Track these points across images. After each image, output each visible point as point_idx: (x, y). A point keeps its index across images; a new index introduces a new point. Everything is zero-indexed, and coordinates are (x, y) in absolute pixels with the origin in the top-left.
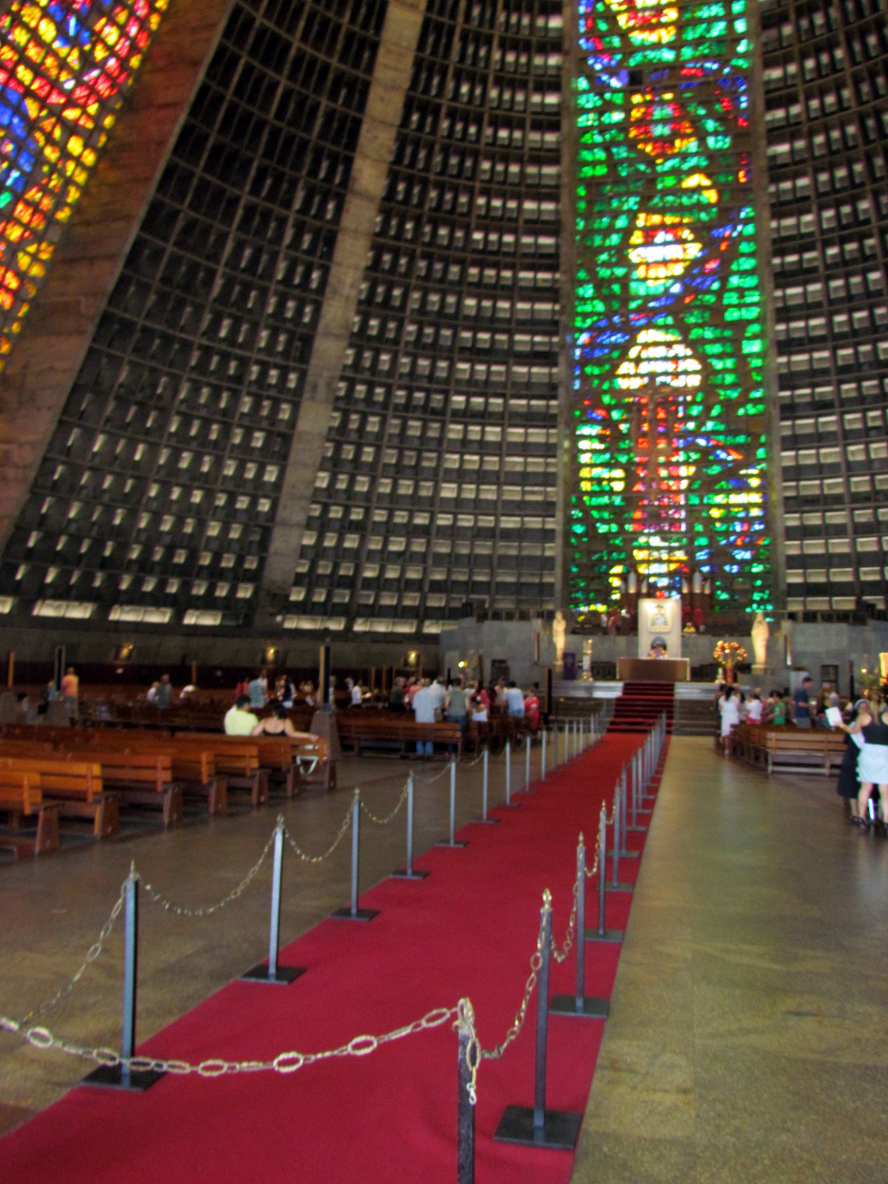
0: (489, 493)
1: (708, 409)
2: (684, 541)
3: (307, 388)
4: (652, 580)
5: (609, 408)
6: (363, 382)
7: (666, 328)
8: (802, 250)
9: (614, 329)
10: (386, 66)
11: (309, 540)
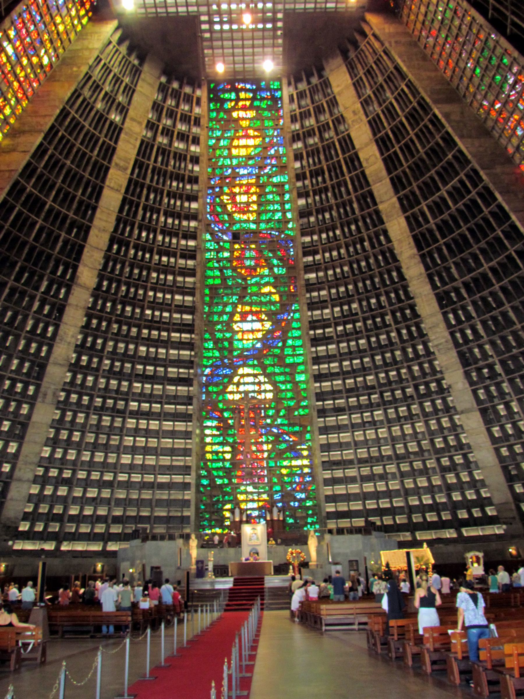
0: (151, 460)
1: (278, 411)
2: (267, 488)
3: (40, 395)
4: (249, 512)
5: (222, 411)
6: (75, 392)
7: (254, 366)
8: (324, 327)
9: (225, 366)
10: (100, 219)
11: (35, 490)
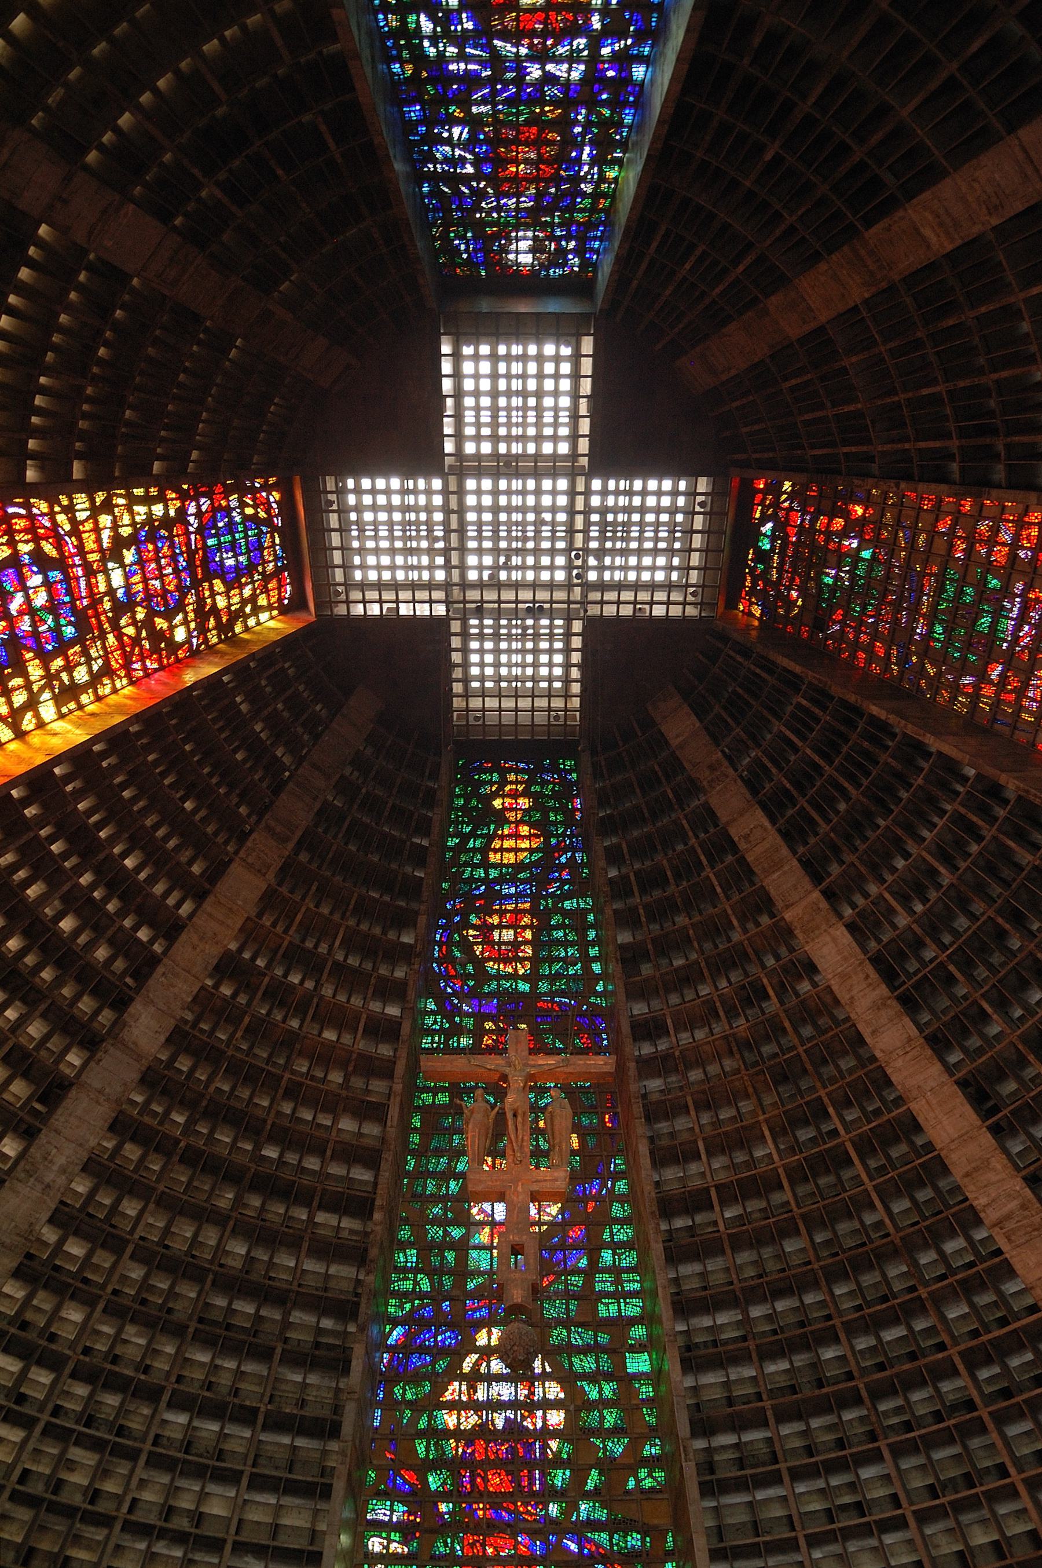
9: (439, 1322)
10: (210, 915)
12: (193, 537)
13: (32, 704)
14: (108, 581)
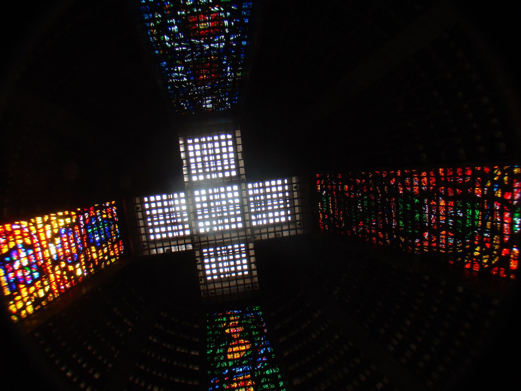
12: (83, 230)
13: (24, 307)
14: (50, 252)
